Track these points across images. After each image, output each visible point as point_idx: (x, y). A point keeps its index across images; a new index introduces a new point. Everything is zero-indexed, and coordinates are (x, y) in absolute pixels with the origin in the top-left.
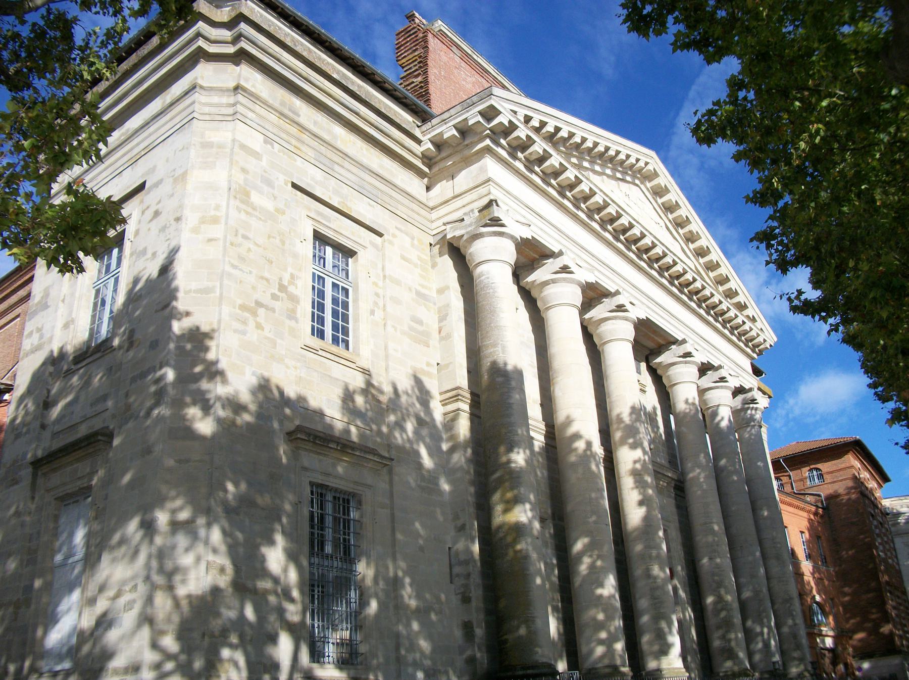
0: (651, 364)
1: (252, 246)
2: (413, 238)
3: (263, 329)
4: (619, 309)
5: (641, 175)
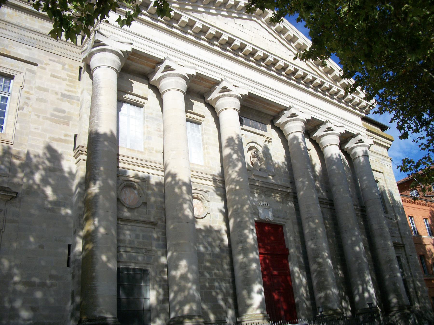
0: (275, 125)
2: (64, 65)
4: (224, 90)
5: (256, 14)
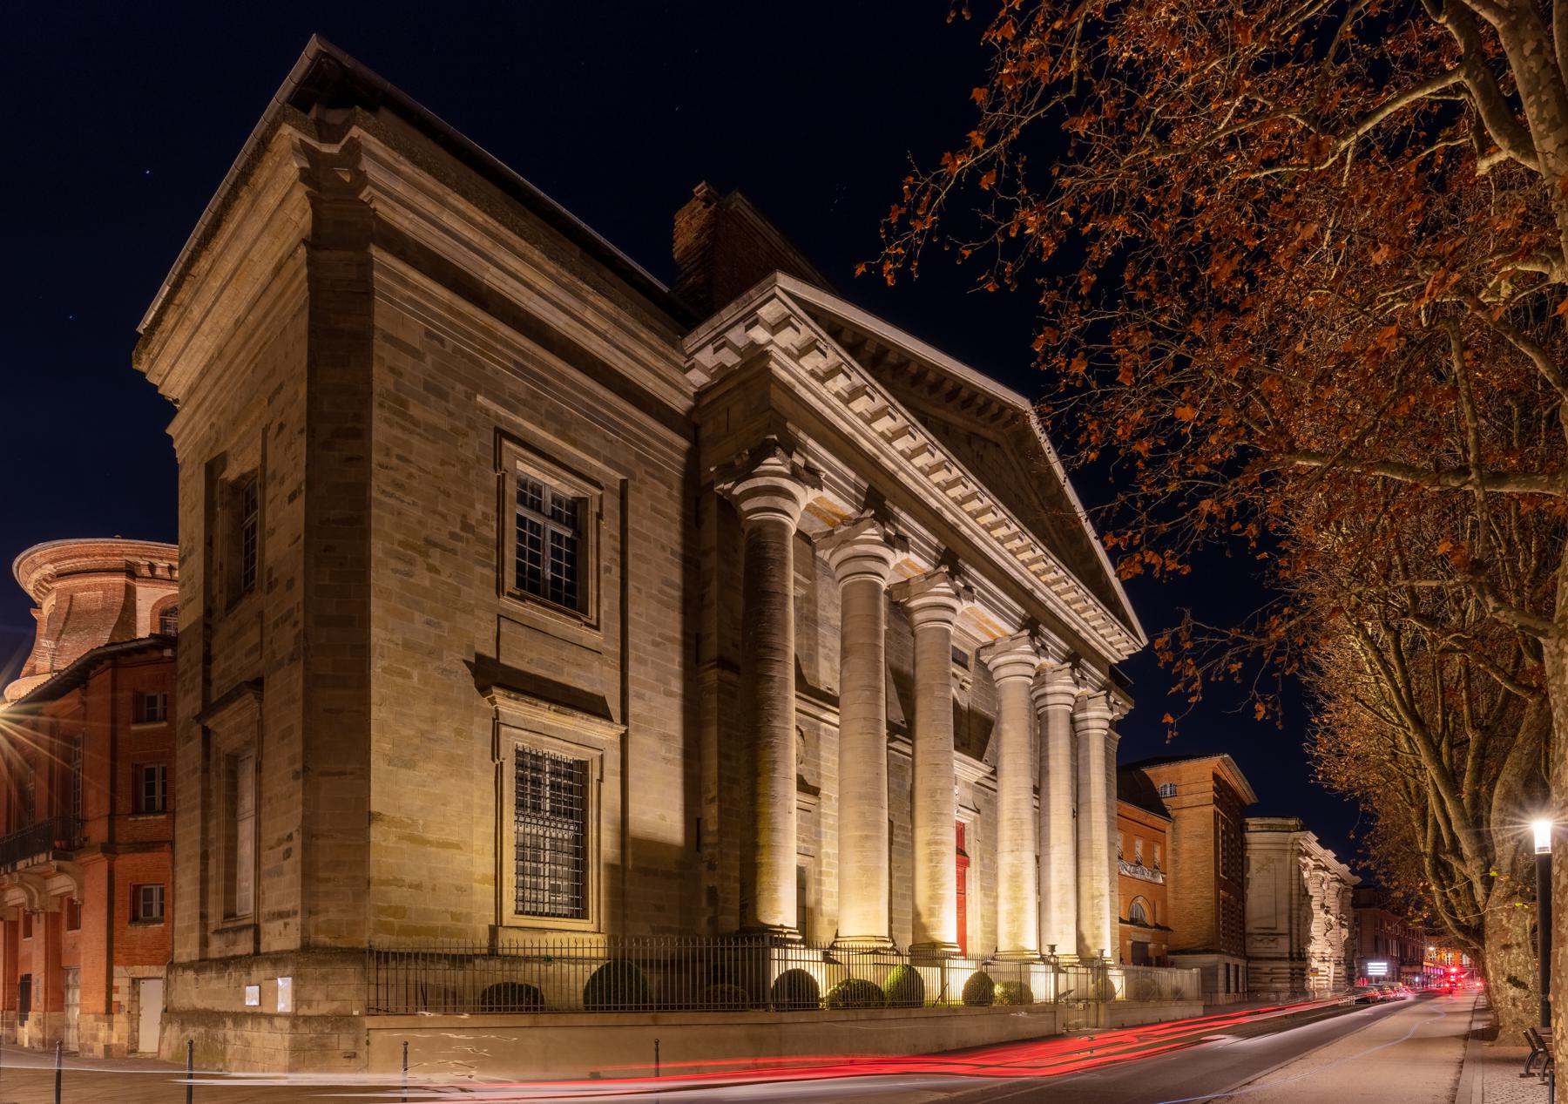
1: (414, 471)
3: (438, 572)
